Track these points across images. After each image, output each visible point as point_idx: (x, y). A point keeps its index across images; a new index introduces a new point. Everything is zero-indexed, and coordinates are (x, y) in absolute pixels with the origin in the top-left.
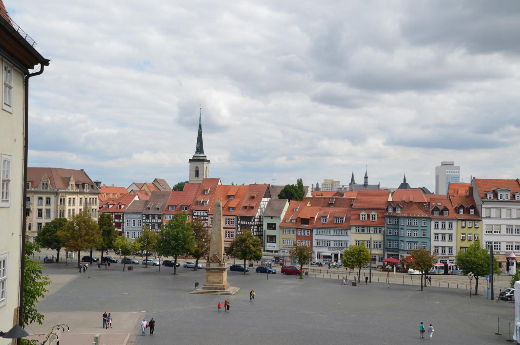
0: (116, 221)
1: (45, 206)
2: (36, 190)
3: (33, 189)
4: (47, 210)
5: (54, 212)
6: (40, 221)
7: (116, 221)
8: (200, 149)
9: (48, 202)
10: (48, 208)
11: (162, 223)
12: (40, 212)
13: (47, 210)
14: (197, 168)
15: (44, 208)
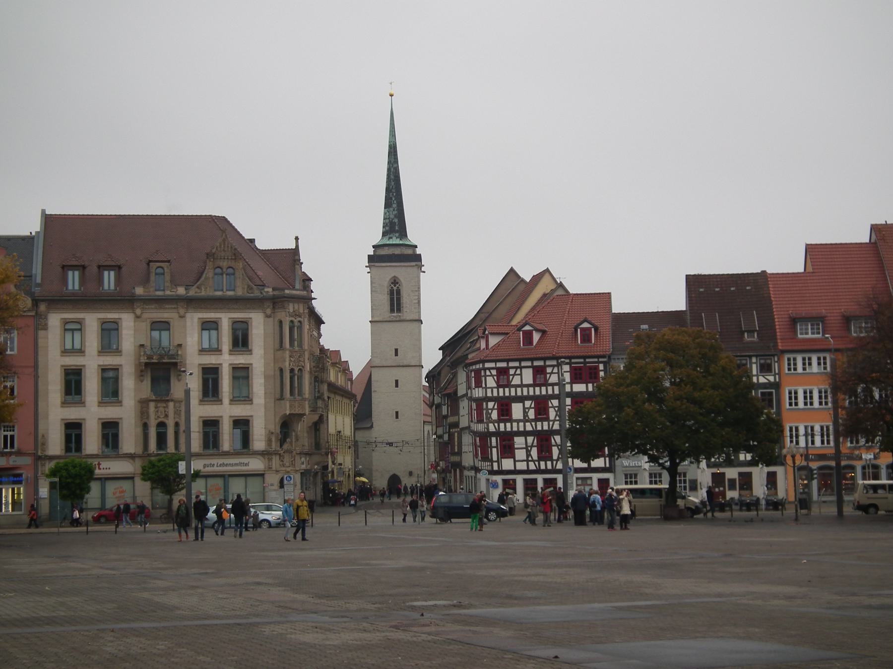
0: (579, 388)
1: (231, 352)
2: (192, 292)
3: (181, 291)
4: (235, 369)
5: (266, 377)
6: (211, 411)
7: (579, 388)
8: (395, 223)
9: (241, 341)
10: (241, 360)
11: (777, 386)
12: (210, 376)
13: (235, 369)
14: (395, 281)
15: (226, 360)
